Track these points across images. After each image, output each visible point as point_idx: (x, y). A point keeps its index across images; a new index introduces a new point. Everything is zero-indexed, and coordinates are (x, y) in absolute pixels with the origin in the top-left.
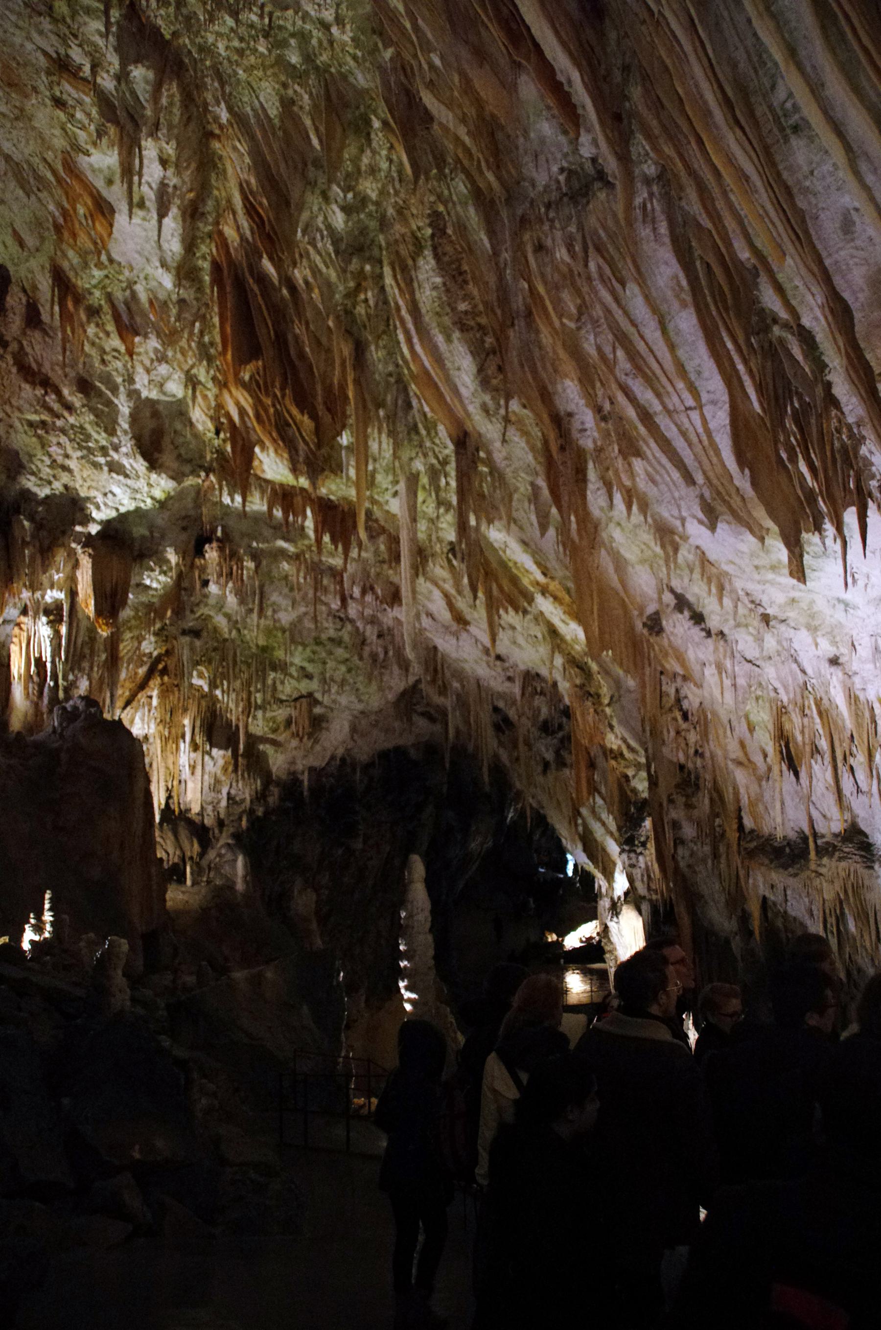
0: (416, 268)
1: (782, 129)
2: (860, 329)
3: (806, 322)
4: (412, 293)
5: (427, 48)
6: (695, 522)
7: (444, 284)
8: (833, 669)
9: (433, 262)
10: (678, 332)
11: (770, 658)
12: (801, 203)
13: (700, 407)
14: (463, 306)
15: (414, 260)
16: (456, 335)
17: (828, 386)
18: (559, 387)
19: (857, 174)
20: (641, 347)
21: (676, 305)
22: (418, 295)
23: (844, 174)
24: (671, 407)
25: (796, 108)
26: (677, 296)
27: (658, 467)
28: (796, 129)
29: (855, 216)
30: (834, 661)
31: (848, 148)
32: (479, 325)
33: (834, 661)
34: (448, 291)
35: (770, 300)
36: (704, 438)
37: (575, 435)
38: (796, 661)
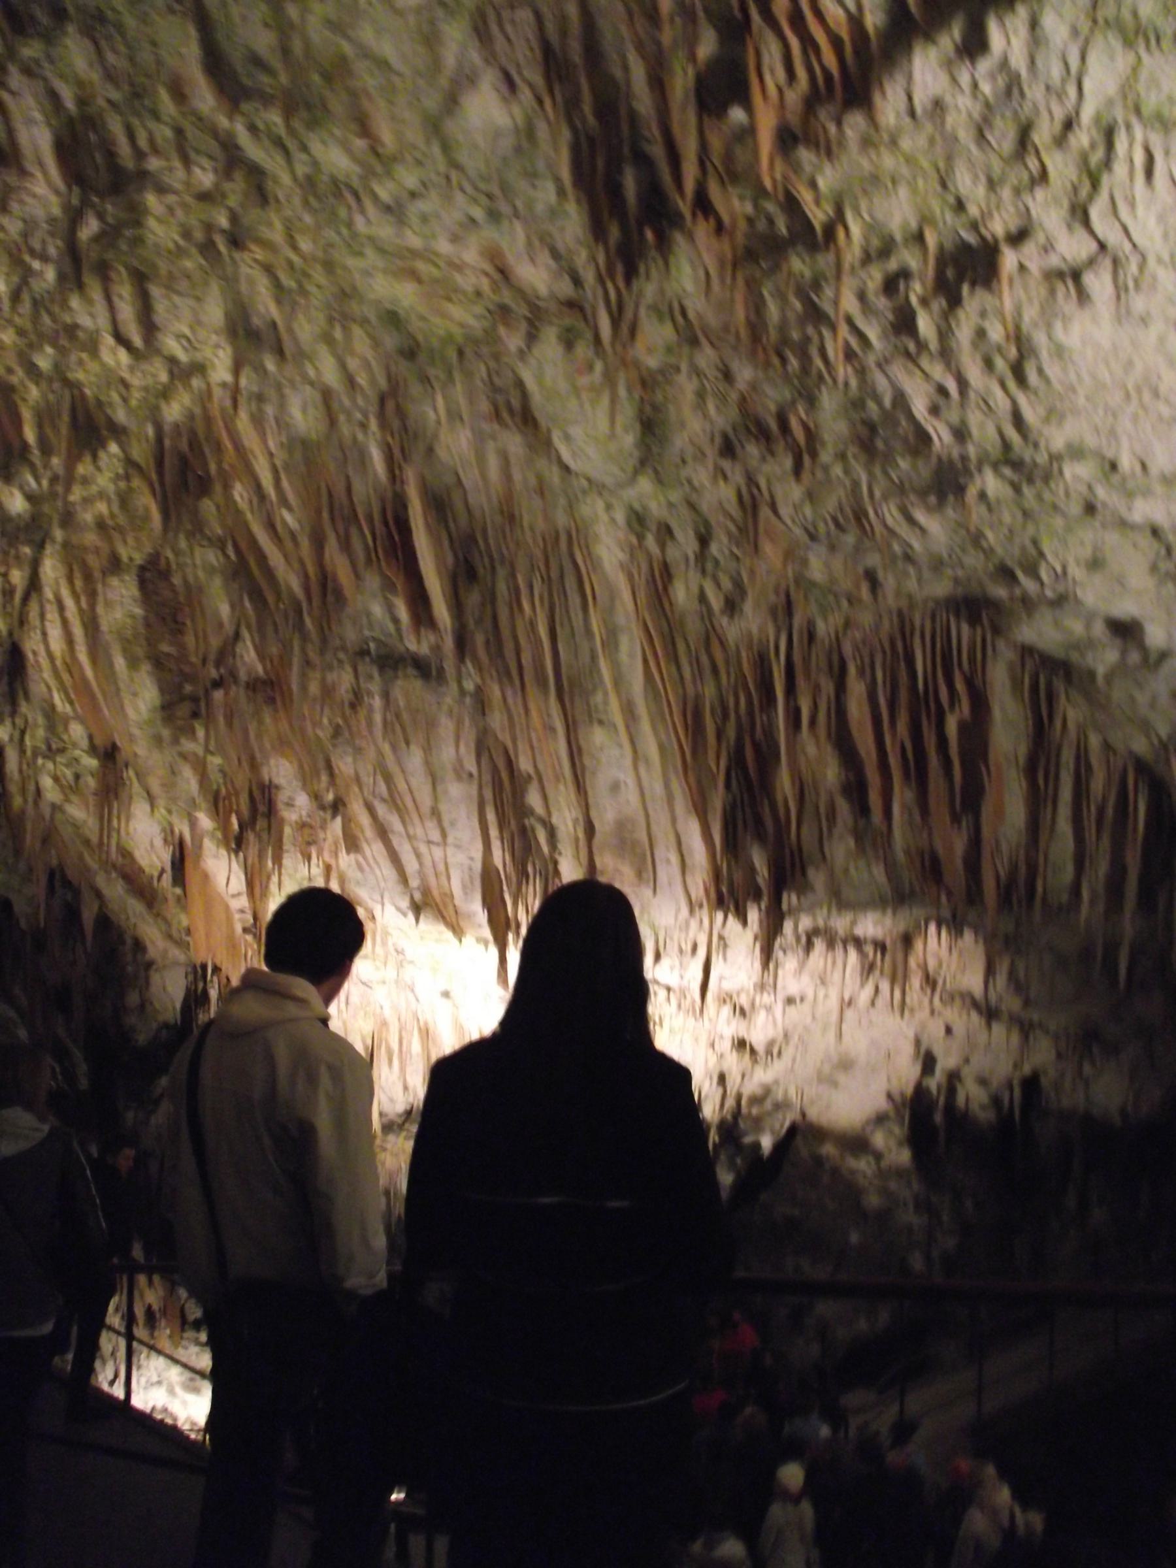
0: (104, 584)
1: (590, 716)
2: (597, 841)
3: (554, 820)
4: (92, 606)
5: (284, 502)
6: (393, 909)
7: (146, 618)
8: (444, 1000)
9: (135, 591)
10: (446, 792)
11: (384, 982)
12: (587, 761)
13: (445, 844)
14: (165, 648)
15: (104, 574)
16: (146, 667)
17: (556, 863)
18: (272, 762)
19: (636, 767)
20: (402, 786)
21: (450, 775)
22: (100, 609)
23: (628, 761)
24: (411, 832)
25: (606, 712)
26: (455, 770)
27: (371, 861)
28: (601, 722)
29: (622, 785)
30: (446, 994)
31: (635, 751)
32: (181, 671)
33: (446, 994)
34: (148, 625)
35: (533, 799)
36: (441, 867)
37: (280, 806)
38: (413, 991)
